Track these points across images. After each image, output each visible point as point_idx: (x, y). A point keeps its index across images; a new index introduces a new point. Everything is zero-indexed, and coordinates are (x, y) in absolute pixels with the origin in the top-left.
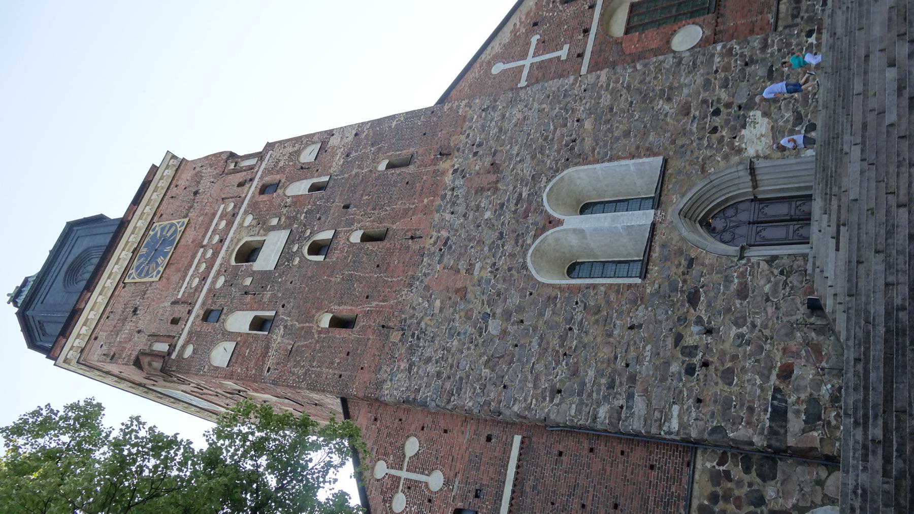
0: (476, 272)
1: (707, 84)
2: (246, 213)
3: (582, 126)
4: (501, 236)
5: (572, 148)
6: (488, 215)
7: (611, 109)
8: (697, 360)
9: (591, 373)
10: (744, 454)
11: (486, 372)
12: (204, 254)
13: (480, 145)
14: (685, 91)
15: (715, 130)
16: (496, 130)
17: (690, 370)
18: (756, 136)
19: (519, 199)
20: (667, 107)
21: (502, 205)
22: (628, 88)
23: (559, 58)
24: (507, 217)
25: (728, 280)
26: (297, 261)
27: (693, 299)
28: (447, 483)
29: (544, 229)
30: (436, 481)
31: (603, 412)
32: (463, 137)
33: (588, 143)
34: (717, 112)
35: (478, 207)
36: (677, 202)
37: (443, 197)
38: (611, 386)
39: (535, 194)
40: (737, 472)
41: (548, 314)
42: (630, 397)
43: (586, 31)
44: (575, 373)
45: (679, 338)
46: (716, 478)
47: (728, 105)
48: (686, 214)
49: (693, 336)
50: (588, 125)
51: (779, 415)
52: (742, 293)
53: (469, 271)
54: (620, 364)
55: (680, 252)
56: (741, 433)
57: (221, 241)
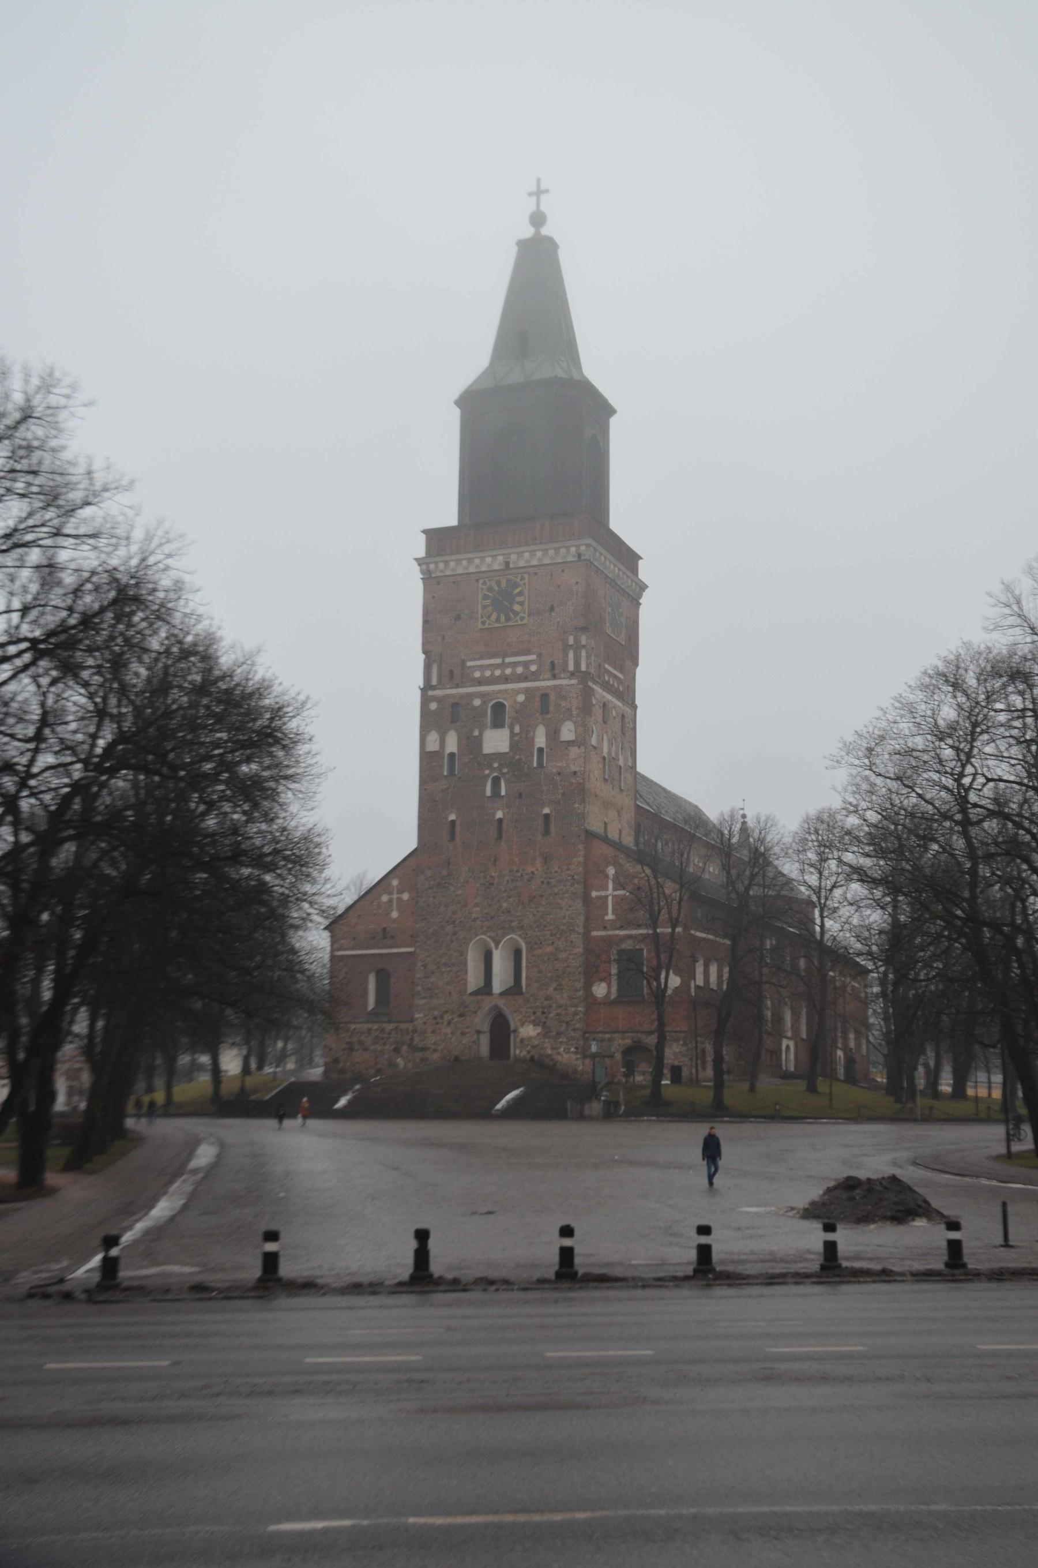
0: (475, 909)
1: (560, 1006)
2: (527, 691)
3: (549, 945)
4: (492, 917)
5: (536, 943)
6: (505, 905)
7: (557, 960)
8: (439, 1020)
9: (432, 980)
10: (412, 1039)
11: (431, 930)
12: (498, 666)
13: (548, 883)
14: (558, 997)
15: (534, 1013)
16: (556, 890)
17: (435, 1018)
18: (529, 1031)
19: (511, 921)
20: (551, 989)
21: (509, 912)
22: (568, 966)
23: (607, 914)
24: (502, 918)
25: (468, 1027)
26: (487, 772)
27: (462, 1015)
28: (395, 920)
29: (494, 941)
30: (395, 914)
31: (419, 988)
32: (556, 869)
33: (539, 952)
34: (543, 1013)
35: (509, 897)
36: (501, 1003)
37: (518, 871)
38: (429, 989)
39: (512, 930)
40: (409, 1037)
41: (455, 954)
42: (424, 998)
43: (621, 928)
44: (433, 973)
45: (446, 1012)
46: (407, 1030)
47: (546, 1018)
48: (496, 1007)
49: (447, 1017)
50: (549, 949)
51: (423, 1049)
52: (463, 1033)
53: (476, 905)
54: (436, 991)
55: (479, 1007)
56: (417, 1039)
57: (506, 680)
